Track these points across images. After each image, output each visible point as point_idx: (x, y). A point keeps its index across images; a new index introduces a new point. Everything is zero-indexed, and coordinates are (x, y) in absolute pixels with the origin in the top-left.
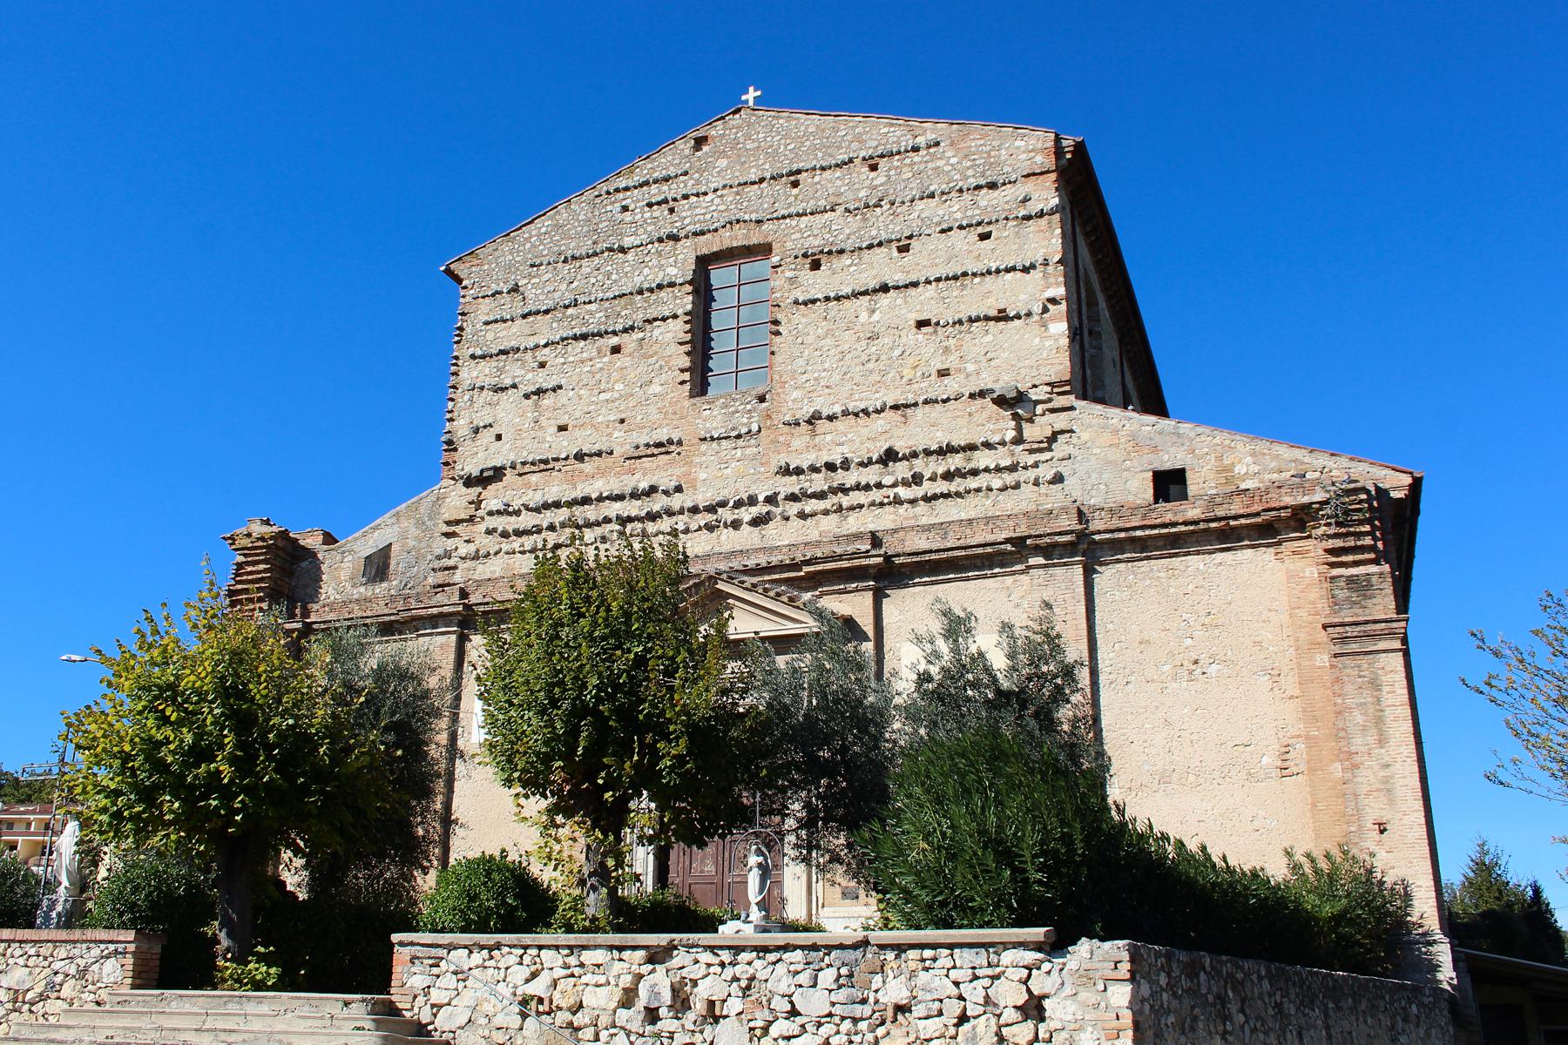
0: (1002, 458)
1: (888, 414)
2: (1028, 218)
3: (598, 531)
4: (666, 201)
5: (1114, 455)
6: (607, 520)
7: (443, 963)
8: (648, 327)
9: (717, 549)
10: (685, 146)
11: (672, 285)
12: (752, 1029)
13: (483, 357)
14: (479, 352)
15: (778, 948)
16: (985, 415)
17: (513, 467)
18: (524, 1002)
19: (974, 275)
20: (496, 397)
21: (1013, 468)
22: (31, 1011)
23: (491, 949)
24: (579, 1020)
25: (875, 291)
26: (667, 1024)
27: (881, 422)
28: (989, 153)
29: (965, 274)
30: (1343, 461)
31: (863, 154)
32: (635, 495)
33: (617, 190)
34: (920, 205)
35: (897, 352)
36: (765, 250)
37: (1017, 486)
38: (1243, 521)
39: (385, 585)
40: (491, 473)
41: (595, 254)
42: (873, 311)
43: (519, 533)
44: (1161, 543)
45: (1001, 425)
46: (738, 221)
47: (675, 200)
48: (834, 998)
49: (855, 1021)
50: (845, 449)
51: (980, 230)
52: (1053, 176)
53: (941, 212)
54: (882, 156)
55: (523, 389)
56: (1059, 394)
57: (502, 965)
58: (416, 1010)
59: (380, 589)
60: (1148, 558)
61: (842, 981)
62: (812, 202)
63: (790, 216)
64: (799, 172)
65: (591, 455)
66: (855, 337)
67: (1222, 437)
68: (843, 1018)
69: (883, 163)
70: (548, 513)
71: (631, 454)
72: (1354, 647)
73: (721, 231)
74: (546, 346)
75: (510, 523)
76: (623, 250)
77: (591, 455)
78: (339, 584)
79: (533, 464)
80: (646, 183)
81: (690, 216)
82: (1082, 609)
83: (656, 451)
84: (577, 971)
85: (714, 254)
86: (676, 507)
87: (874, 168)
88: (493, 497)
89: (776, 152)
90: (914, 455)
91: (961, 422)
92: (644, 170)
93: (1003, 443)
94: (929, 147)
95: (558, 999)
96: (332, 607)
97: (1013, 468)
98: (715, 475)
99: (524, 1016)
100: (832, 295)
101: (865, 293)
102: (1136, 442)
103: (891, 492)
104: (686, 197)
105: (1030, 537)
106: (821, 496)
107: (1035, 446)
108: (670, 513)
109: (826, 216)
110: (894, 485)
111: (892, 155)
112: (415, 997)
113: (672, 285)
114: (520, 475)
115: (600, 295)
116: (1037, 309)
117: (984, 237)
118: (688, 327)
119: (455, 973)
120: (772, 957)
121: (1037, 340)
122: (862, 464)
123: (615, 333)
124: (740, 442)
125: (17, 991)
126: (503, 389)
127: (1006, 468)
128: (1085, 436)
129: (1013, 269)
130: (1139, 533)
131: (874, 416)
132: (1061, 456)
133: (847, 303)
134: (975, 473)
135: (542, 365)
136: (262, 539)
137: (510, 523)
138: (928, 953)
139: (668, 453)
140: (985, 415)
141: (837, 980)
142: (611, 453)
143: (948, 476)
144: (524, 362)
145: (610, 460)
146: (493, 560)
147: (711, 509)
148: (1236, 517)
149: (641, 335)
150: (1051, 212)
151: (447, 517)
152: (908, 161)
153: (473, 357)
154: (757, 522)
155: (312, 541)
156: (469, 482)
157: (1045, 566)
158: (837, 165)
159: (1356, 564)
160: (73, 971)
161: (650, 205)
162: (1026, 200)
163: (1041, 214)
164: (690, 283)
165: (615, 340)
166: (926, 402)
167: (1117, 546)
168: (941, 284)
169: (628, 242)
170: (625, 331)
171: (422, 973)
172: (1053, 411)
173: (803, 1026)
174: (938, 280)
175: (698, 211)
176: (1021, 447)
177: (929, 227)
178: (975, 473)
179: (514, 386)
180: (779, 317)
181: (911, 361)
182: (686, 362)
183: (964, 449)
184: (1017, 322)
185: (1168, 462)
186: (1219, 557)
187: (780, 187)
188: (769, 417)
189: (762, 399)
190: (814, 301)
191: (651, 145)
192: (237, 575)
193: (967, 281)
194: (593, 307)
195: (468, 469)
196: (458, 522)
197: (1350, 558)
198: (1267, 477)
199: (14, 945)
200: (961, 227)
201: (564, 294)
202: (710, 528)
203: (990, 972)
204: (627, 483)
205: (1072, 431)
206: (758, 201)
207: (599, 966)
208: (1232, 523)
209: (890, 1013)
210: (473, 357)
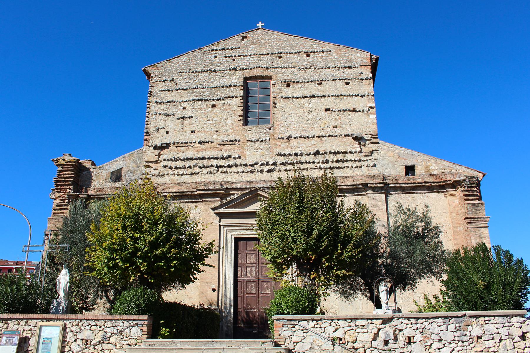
0: (355, 157)
1: (316, 139)
2: (362, 79)
3: (208, 170)
4: (232, 56)
5: (393, 159)
6: (212, 166)
7: (297, 327)
8: (226, 99)
9: (254, 179)
10: (238, 38)
11: (235, 86)
12: (426, 346)
13: (160, 103)
14: (159, 101)
15: (432, 318)
16: (349, 142)
17: (174, 144)
18: (334, 339)
19: (345, 96)
20: (166, 118)
21: (359, 161)
22: (95, 349)
23: (317, 320)
24: (356, 345)
25: (310, 97)
26: (392, 345)
27: (313, 141)
28: (348, 56)
29: (341, 95)
30: (463, 168)
31: (304, 50)
32: (222, 158)
33: (213, 50)
35: (318, 118)
36: (270, 78)
37: (361, 167)
38: (436, 184)
39: (120, 183)
40: (165, 145)
41: (204, 71)
42: (310, 104)
43: (176, 168)
44: (409, 189)
45: (355, 146)
46: (260, 67)
47: (235, 56)
48: (455, 334)
49: (463, 342)
50: (301, 149)
51: (346, 81)
52: (370, 67)
53: (332, 74)
54: (311, 52)
55: (177, 116)
56: (374, 138)
57: (323, 326)
58: (286, 344)
59: (118, 184)
60: (405, 193)
61: (457, 328)
62: (286, 64)
63: (279, 68)
64: (281, 53)
65: (205, 142)
66: (303, 112)
67: (426, 157)
68: (459, 341)
69: (311, 54)
70: (188, 161)
71: (220, 143)
72: (474, 225)
73: (253, 69)
74: (186, 102)
75: (174, 164)
76: (215, 71)
77: (205, 142)
78: (100, 180)
79: (182, 143)
80: (224, 49)
81: (240, 63)
82: (385, 208)
83: (230, 143)
84: (354, 328)
85: (250, 77)
86: (239, 163)
87: (308, 56)
88: (166, 154)
89: (273, 45)
90: (326, 153)
91: (341, 143)
92: (223, 44)
93: (356, 152)
94: (328, 51)
95: (347, 338)
96: (98, 189)
97: (359, 161)
98: (253, 154)
99: (334, 345)
100: (295, 96)
101: (307, 97)
102: (399, 156)
103: (318, 165)
104: (239, 56)
105: (369, 184)
107: (367, 154)
109: (292, 69)
110: (319, 163)
111: (314, 52)
112: (285, 340)
113: (235, 86)
114: (176, 147)
115: (207, 86)
116: (366, 109)
117: (347, 84)
118: (242, 101)
119: (302, 330)
120: (431, 321)
121: (366, 120)
122: (307, 155)
123: (213, 100)
124: (262, 143)
125: (87, 341)
126: (169, 115)
127: (357, 160)
128: (383, 152)
129: (358, 95)
130: (403, 185)
131: (311, 139)
132: (375, 158)
133: (300, 100)
134: (347, 161)
135: (184, 108)
136: (70, 162)
137: (174, 164)
138: (487, 319)
139: (235, 144)
140: (349, 142)
141: (455, 328)
142: (213, 142)
143: (337, 161)
144: (177, 107)
145: (212, 145)
146: (166, 177)
147: (252, 165)
148: (434, 183)
149: (223, 102)
151: (146, 159)
152: (320, 55)
153: (156, 102)
154: (269, 171)
155: (87, 164)
156: (156, 148)
157: (373, 193)
158: (295, 53)
159: (473, 200)
160: (115, 331)
161: (226, 57)
162: (361, 74)
163: (366, 79)
164: (242, 86)
165: (213, 103)
166: (329, 136)
167: (395, 189)
168: (333, 98)
169: (217, 69)
170: (217, 100)
171: (288, 330)
172: (372, 143)
173: (444, 345)
174: (332, 96)
175: (244, 61)
176: (362, 154)
177: (328, 78)
178: (347, 161)
179: (173, 115)
180: (276, 101)
181: (323, 122)
182: (241, 113)
183: (343, 153)
184: (359, 113)
185: (409, 163)
186: (427, 194)
187: (275, 57)
188: (273, 135)
189: (270, 129)
190: (288, 98)
191: (226, 36)
192: (59, 175)
193: (342, 97)
194: (204, 90)
195: (154, 143)
196: (150, 162)
197: (471, 198)
198: (440, 171)
199: (83, 321)
200: (339, 80)
202: (252, 172)
203: (509, 324)
204: (220, 154)
205: (378, 150)
206: (267, 61)
207: (363, 326)
208: (432, 184)
209: (476, 339)
210: (156, 102)
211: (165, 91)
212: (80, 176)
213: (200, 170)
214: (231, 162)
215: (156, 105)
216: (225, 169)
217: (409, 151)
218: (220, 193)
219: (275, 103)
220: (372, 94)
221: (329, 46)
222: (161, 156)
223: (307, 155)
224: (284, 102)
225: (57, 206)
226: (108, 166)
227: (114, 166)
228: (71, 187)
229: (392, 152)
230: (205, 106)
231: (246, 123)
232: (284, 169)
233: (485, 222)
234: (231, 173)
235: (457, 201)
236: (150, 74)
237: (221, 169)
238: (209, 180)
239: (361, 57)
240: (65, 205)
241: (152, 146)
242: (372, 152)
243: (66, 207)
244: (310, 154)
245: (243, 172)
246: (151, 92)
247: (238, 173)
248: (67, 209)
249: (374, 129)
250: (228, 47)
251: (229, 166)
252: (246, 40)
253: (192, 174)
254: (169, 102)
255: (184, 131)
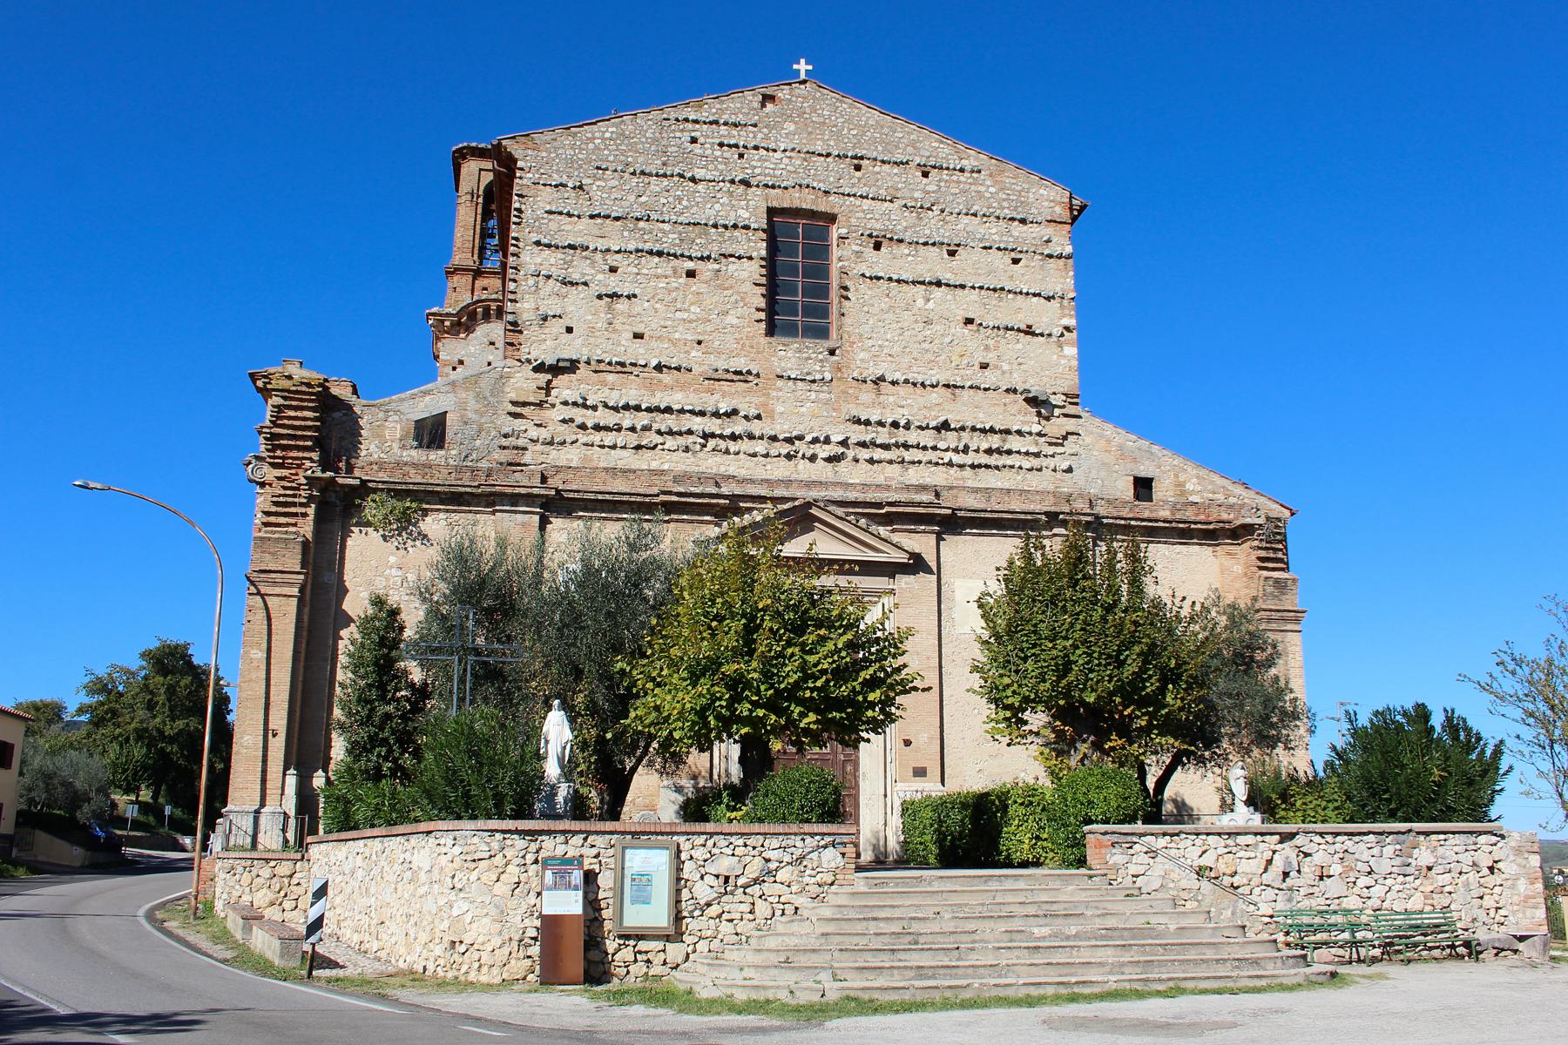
1: (940, 390)
2: (1050, 256)
4: (736, 146)
5: (1110, 459)
6: (690, 432)
10: (753, 99)
11: (746, 227)
13: (549, 246)
16: (1016, 407)
17: (588, 363)
20: (565, 289)
21: (1037, 455)
25: (930, 283)
29: (1002, 289)
30: (1251, 494)
32: (716, 414)
33: (686, 120)
34: (966, 220)
35: (947, 340)
36: (832, 218)
39: (441, 453)
40: (567, 364)
41: (665, 176)
43: (597, 428)
45: (1028, 418)
47: (745, 147)
51: (1013, 255)
54: (934, 167)
55: (595, 289)
59: (435, 456)
64: (862, 158)
70: (627, 414)
76: (693, 180)
79: (610, 364)
80: (716, 122)
81: (758, 167)
87: (925, 175)
88: (566, 388)
90: (963, 429)
96: (381, 465)
97: (1037, 455)
98: (792, 411)
101: (922, 283)
102: (1123, 454)
104: (756, 148)
106: (886, 447)
108: (751, 437)
110: (947, 450)
111: (941, 168)
113: (746, 227)
115: (674, 218)
116: (1056, 331)
117: (1016, 261)
122: (920, 427)
123: (690, 258)
124: (814, 386)
126: (572, 284)
128: (1088, 440)
129: (1039, 295)
133: (905, 286)
134: (1009, 452)
135: (613, 270)
136: (309, 385)
140: (1016, 407)
143: (989, 451)
144: (594, 262)
145: (689, 375)
147: (789, 441)
149: (717, 266)
150: (1068, 257)
151: (513, 396)
153: (538, 243)
154: (829, 460)
155: (341, 390)
156: (540, 368)
161: (721, 145)
162: (1049, 241)
163: (1060, 257)
165: (690, 265)
169: (700, 173)
170: (702, 259)
172: (1066, 415)
178: (1009, 452)
179: (585, 284)
180: (848, 283)
181: (958, 350)
183: (1001, 432)
187: (845, 166)
188: (839, 369)
190: (878, 278)
191: (723, 86)
194: (666, 227)
196: (524, 404)
201: (630, 205)
202: (789, 457)
211: (561, 213)
212: (333, 428)
213: (659, 439)
214: (739, 427)
215: (536, 249)
216: (722, 445)
217: (1144, 444)
218: (717, 505)
219: (846, 288)
220: (1072, 295)
221: (976, 159)
222: (554, 392)
223: (920, 427)
224: (865, 286)
225: (276, 504)
226: (406, 404)
227: (422, 405)
228: (315, 456)
229: (1108, 441)
230: (670, 272)
231: (771, 331)
232: (867, 457)
233: (1297, 621)
234: (738, 453)
235: (1238, 569)
236: (515, 161)
237: (712, 443)
238: (681, 468)
239: (1049, 198)
240: (302, 505)
241: (529, 361)
242: (1065, 438)
243: (303, 510)
244: (927, 427)
245: (766, 456)
246: (519, 210)
247: (754, 455)
248: (305, 515)
249: (1070, 382)
250: (726, 117)
251: (734, 437)
252: (770, 107)
253: (638, 447)
254: (571, 247)
255: (615, 331)
